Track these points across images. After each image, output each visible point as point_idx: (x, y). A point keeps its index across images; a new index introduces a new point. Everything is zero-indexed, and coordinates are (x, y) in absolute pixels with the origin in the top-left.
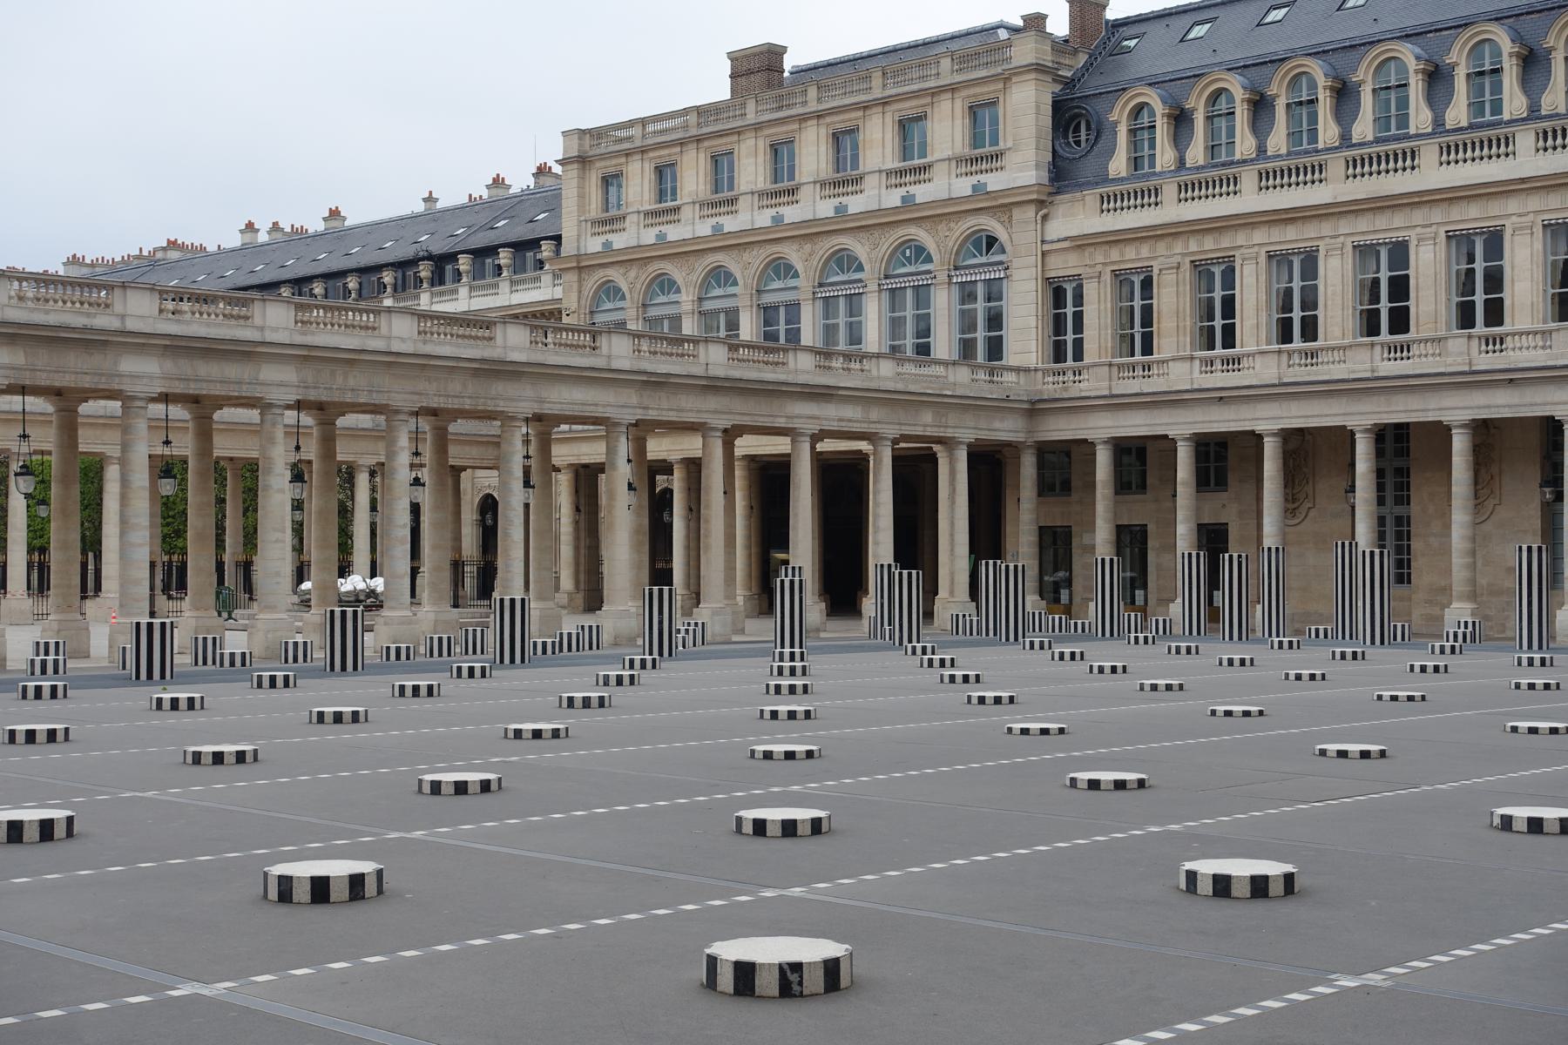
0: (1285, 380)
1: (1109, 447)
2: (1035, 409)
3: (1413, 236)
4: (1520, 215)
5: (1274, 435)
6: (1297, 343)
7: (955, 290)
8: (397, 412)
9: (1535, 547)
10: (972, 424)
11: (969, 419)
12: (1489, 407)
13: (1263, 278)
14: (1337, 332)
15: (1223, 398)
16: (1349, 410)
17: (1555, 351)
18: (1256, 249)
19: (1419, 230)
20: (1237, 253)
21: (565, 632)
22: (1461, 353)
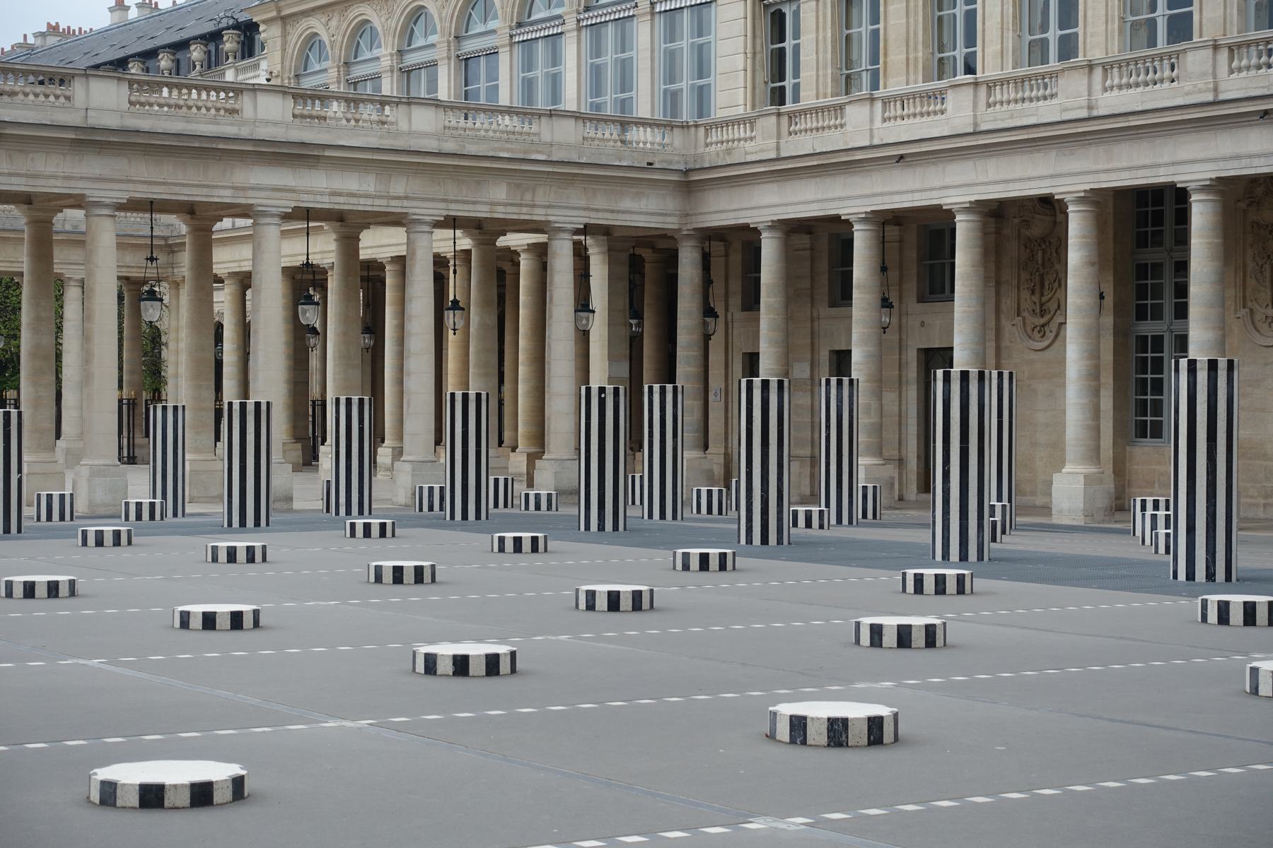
0: (984, 127)
1: (778, 234)
2: (690, 183)
7: (660, 22)
8: (264, 214)
9: (355, 399)
10: (583, 203)
11: (576, 197)
12: (1237, 157)
15: (902, 158)
16: (1059, 170)
21: (133, 501)
22: (1204, 74)
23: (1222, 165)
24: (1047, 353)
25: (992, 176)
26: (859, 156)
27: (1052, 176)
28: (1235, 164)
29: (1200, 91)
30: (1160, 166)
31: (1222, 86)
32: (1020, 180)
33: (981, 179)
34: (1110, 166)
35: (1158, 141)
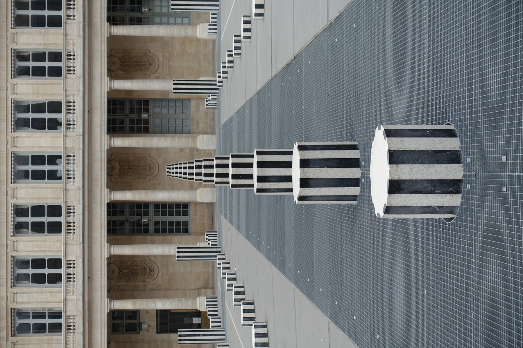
3: (12, 201)
4: (7, 143)
5: (110, 247)
6: (62, 271)
12: (101, 125)
13: (25, 290)
14: (58, 244)
16: (99, 203)
17: (76, 93)
18: (9, 294)
19: (9, 198)
20: (11, 306)
23: (103, 132)
24: (160, 267)
25: (99, 235)
26: (87, 275)
27: (101, 205)
28: (103, 127)
29: (79, 141)
30: (101, 157)
31: (78, 134)
32: (101, 220)
33: (99, 240)
34: (100, 179)
35: (93, 159)
